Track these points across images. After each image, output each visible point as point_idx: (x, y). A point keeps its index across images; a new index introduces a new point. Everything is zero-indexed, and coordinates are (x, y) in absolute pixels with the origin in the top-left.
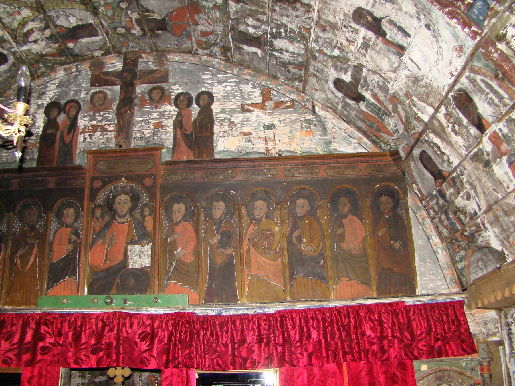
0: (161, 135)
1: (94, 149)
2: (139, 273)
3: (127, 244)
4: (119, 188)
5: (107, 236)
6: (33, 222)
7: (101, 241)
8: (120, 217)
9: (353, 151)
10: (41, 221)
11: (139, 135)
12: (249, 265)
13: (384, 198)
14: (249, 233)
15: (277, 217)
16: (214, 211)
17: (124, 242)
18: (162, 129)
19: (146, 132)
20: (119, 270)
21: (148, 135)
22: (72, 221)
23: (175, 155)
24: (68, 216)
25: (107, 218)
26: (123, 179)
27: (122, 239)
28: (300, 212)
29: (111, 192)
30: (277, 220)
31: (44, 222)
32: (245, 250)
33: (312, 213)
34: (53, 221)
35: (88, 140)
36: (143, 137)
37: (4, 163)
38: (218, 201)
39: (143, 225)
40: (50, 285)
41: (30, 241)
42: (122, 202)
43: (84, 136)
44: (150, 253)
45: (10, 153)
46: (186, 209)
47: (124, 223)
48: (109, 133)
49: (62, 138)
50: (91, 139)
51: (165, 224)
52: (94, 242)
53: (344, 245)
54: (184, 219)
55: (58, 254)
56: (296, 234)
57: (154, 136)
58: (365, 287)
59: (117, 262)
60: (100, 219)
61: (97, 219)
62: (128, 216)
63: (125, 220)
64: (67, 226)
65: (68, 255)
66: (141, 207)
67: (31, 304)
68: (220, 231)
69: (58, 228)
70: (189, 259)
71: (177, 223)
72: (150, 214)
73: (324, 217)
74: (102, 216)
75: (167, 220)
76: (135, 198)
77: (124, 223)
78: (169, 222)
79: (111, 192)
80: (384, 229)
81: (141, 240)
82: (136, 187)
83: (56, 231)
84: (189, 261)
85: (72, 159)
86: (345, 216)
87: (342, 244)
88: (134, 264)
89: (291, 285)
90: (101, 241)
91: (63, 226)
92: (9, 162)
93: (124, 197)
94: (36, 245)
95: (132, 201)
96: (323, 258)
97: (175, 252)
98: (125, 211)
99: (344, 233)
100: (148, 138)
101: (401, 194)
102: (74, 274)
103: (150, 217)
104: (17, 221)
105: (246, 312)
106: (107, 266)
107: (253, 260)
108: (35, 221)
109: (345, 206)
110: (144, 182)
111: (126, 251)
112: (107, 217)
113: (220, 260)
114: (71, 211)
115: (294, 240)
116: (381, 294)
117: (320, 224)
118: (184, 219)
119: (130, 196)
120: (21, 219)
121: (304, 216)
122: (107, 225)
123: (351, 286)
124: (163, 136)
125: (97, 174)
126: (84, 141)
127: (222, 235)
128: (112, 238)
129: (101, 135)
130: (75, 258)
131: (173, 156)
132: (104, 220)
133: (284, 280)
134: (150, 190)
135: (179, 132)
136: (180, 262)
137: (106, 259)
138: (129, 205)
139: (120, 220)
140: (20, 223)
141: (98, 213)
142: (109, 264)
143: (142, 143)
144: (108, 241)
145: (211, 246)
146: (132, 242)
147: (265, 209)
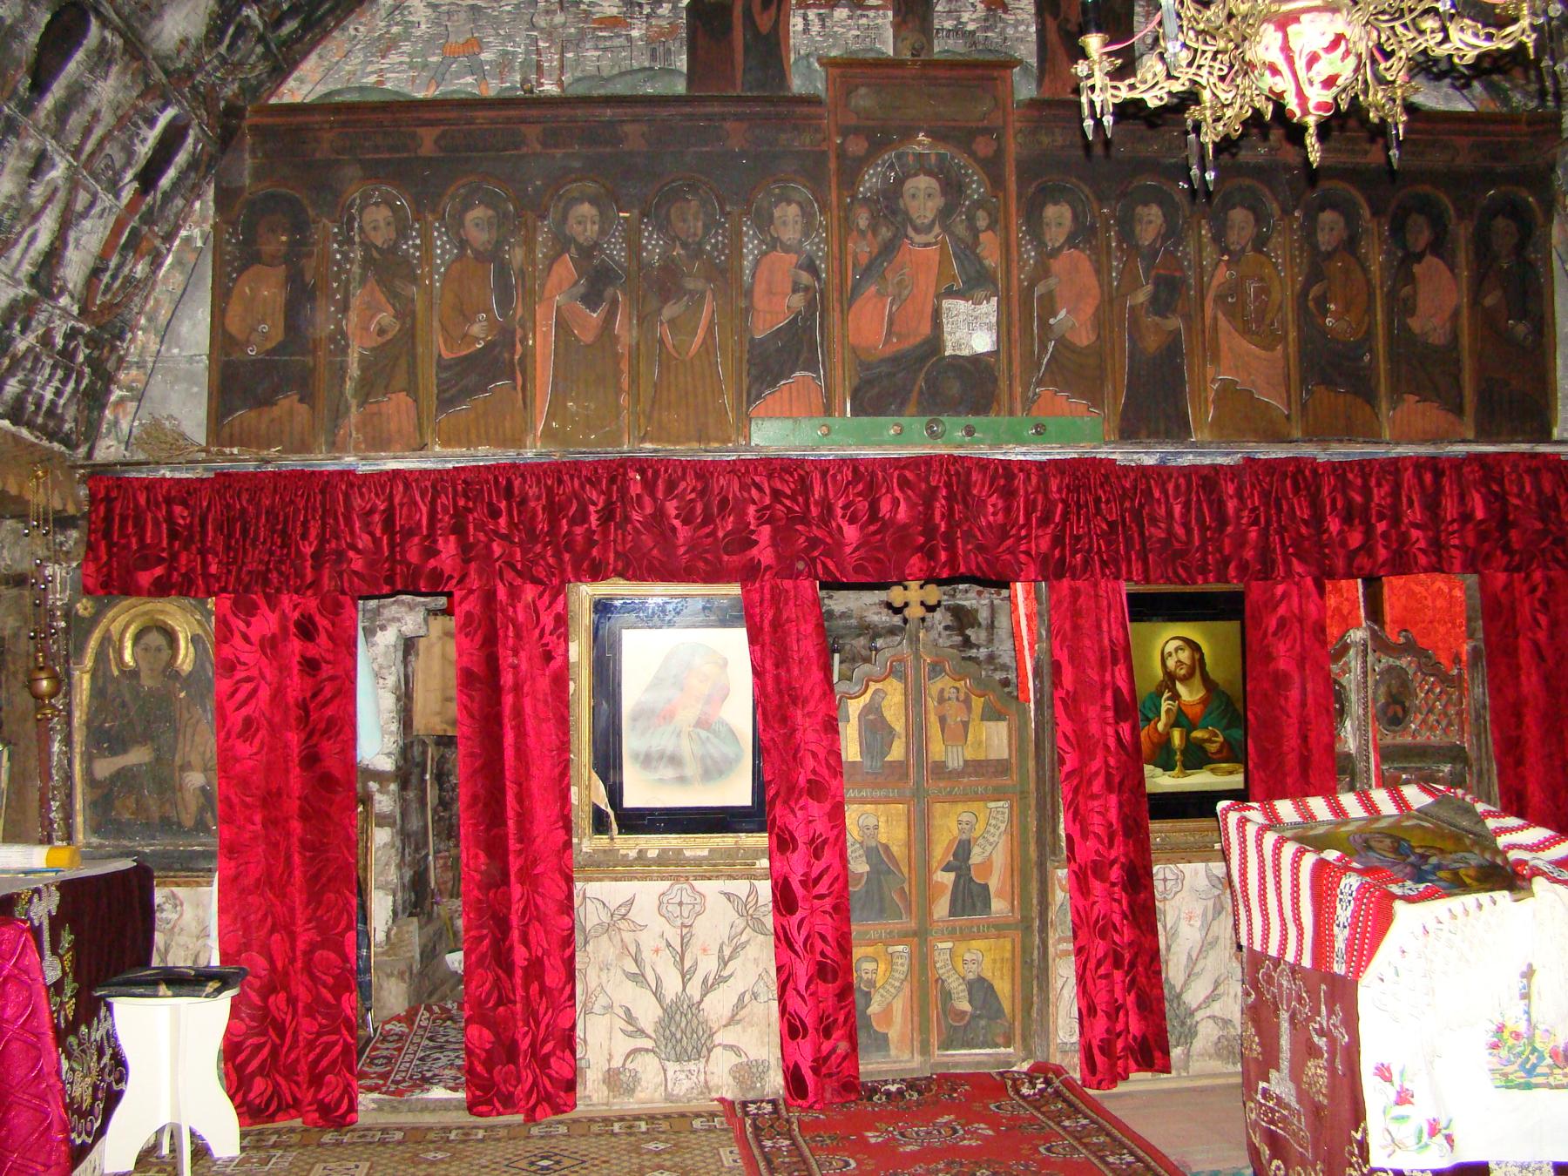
0: (1003, 29)
1: (833, 54)
2: (968, 366)
3: (939, 297)
4: (911, 159)
5: (889, 276)
6: (695, 235)
7: (873, 289)
8: (917, 230)
9: (1441, 106)
10: (717, 233)
11: (948, 24)
12: (1215, 357)
13: (1501, 223)
14: (1215, 283)
15: (1275, 250)
16: (1138, 229)
17: (932, 290)
18: (1006, 10)
19: (965, 17)
20: (923, 359)
21: (971, 27)
22: (798, 236)
23: (1046, 80)
24: (784, 223)
25: (885, 233)
26: (921, 137)
27: (926, 284)
28: (1325, 240)
29: (891, 167)
30: (1277, 257)
31: (724, 236)
32: (1208, 321)
33: (1351, 244)
34: (747, 233)
35: (815, 28)
36: (958, 31)
37: (592, 77)
38: (1146, 204)
39: (973, 252)
40: (754, 392)
41: (690, 284)
42: (921, 195)
43: (805, 18)
44: (994, 320)
45: (605, 49)
46: (1075, 217)
47: (927, 245)
48: (872, 14)
49: (748, 16)
50: (823, 26)
51: (1027, 252)
52: (856, 287)
53: (1415, 324)
54: (1071, 241)
55: (768, 317)
56: (1315, 291)
57: (986, 29)
58: (1451, 417)
59: (919, 340)
60: (870, 234)
61: (862, 233)
62: (937, 229)
63: (930, 238)
64: (787, 249)
65: (795, 319)
66: (969, 208)
67: (709, 441)
68: (1153, 273)
69: (764, 254)
70: (1084, 338)
71: (1056, 252)
72: (990, 227)
73: (1377, 259)
74: (874, 228)
75: (1031, 241)
76: (952, 187)
77: (927, 245)
78: (1035, 248)
79: (891, 167)
80: (1498, 293)
81: (971, 289)
82: (953, 158)
83: (757, 262)
84: (1085, 343)
85: (781, 76)
86: (1419, 257)
87: (1409, 321)
88: (958, 345)
89: (1304, 406)
90: (873, 289)
91: (774, 248)
92: (605, 74)
93: (923, 182)
94: (709, 296)
95: (944, 193)
96: (1371, 351)
97: (1052, 321)
98: (930, 215)
99: (1415, 292)
100: (973, 33)
101: (1540, 216)
102: (811, 365)
103: (990, 233)
104: (651, 234)
105: (1220, 460)
106: (889, 351)
107: (1224, 346)
108: (700, 232)
109: (1421, 235)
110: (974, 147)
111: (937, 314)
112: (884, 230)
113: (1152, 343)
114: (793, 210)
115: (1311, 304)
116: (1483, 435)
117: (1365, 270)
118: (1071, 241)
119: (938, 180)
120: (663, 227)
121: (1335, 250)
122: (889, 249)
123: (1424, 414)
124: (1010, 31)
125: (853, 121)
126: (806, 30)
127: (1156, 285)
128: (900, 282)
129: (850, 17)
130: (812, 329)
131: (1040, 82)
132: (880, 238)
133: (1288, 391)
134: (992, 168)
135: (1051, 25)
136: (1062, 342)
137: (889, 333)
138: (939, 202)
139: (918, 238)
140: (659, 238)
141: (863, 221)
142: (896, 346)
143: (957, 46)
144: (890, 289)
145: (1132, 308)
146: (951, 293)
147: (1250, 231)
